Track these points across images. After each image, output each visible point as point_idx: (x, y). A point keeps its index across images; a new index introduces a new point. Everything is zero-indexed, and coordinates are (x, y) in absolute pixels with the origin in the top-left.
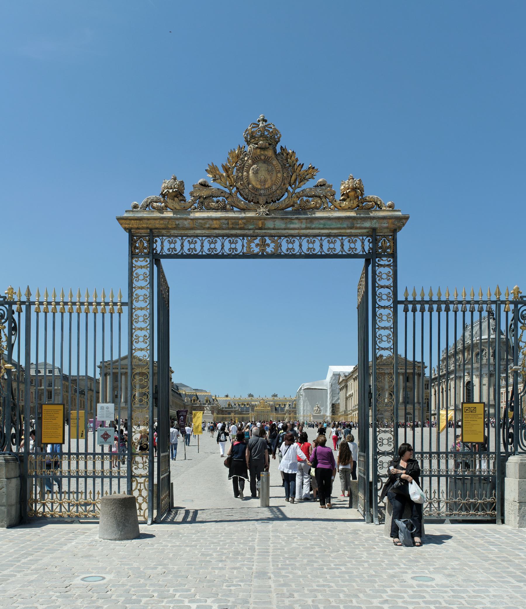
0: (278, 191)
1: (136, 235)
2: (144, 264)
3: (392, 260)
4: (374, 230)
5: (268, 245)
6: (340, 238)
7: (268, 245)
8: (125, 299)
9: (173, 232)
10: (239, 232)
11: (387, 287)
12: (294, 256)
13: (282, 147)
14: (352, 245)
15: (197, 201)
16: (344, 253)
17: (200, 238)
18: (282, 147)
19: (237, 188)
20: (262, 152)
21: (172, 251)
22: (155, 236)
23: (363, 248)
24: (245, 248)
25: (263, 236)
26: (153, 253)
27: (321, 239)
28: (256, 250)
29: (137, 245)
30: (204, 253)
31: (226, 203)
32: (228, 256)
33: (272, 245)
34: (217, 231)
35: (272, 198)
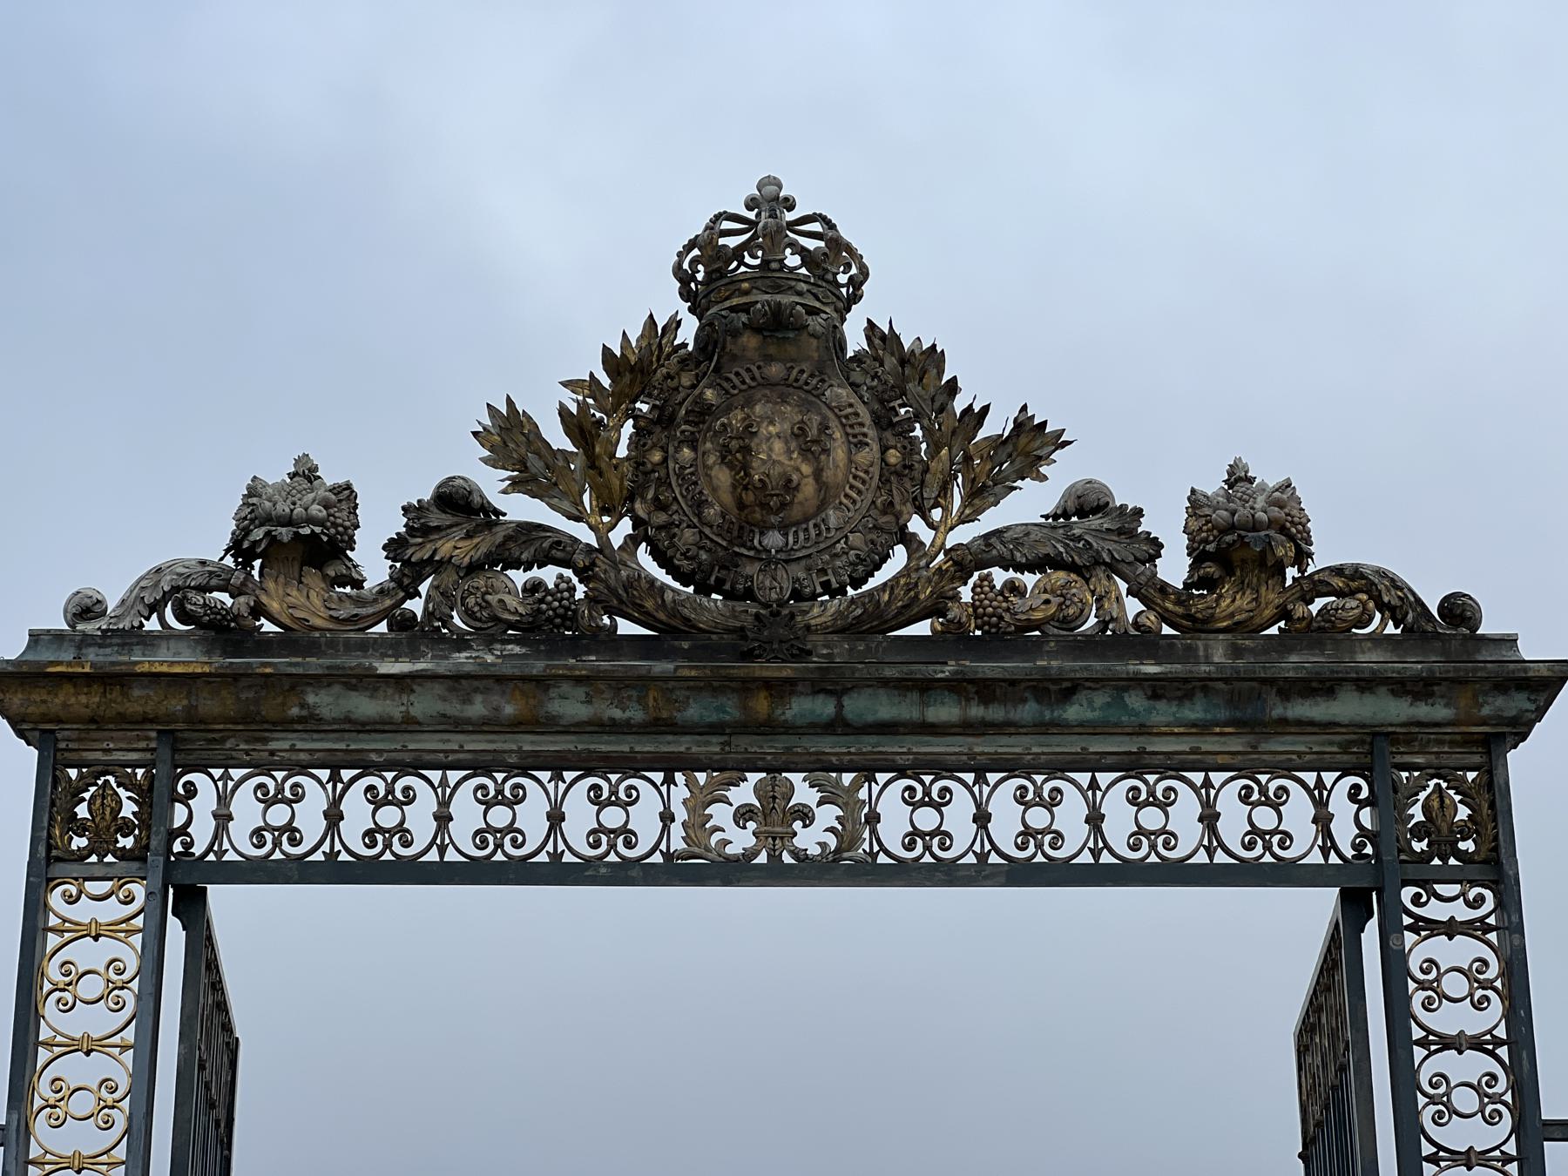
1: (73, 756)
2: (112, 911)
5: (806, 816)
7: (806, 816)
10: (646, 746)
11: (1477, 1044)
12: (948, 874)
13: (871, 326)
14: (1265, 818)
15: (424, 588)
16: (1221, 858)
17: (435, 776)
18: (871, 326)
19: (637, 523)
21: (277, 844)
23: (1328, 834)
24: (677, 830)
26: (170, 850)
28: (741, 840)
29: (82, 811)
30: (451, 856)
31: (579, 595)
32: (585, 873)
33: (828, 815)
34: (529, 743)
35: (823, 571)
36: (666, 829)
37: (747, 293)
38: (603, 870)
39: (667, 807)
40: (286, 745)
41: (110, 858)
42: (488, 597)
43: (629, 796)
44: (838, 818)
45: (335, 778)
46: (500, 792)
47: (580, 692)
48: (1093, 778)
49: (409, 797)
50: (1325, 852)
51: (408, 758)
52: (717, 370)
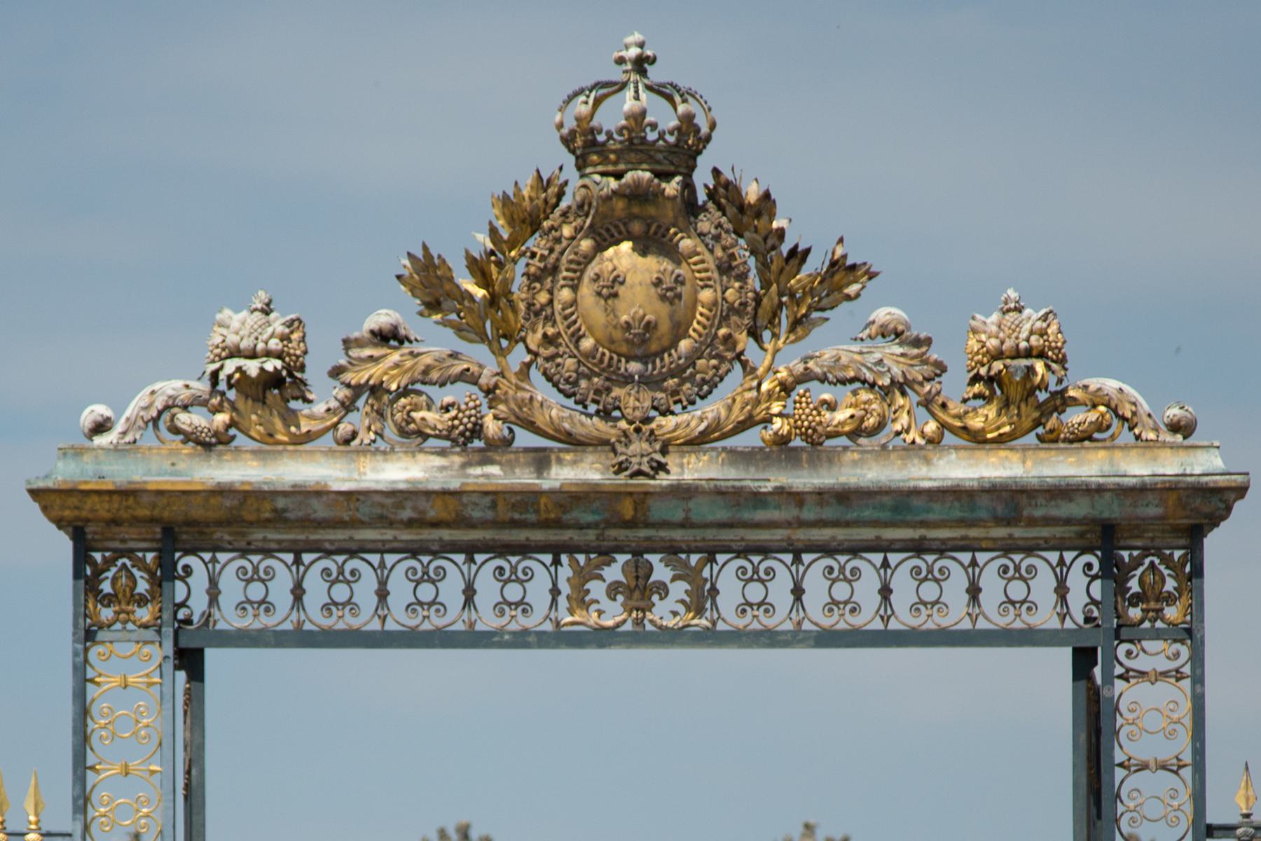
1: (99, 545)
3: (1185, 652)
5: (662, 589)
6: (966, 557)
9: (257, 535)
10: (538, 536)
12: (769, 638)
13: (716, 172)
14: (1017, 590)
15: (360, 403)
16: (982, 624)
17: (375, 558)
18: (716, 172)
20: (636, 210)
22: (187, 552)
24: (562, 601)
25: (637, 553)
27: (885, 564)
33: (679, 590)
34: (447, 534)
36: (554, 601)
37: (615, 163)
38: (507, 637)
39: (555, 584)
41: (130, 626)
42: (413, 414)
43: (526, 574)
44: (686, 592)
45: (298, 561)
46: (426, 573)
48: (885, 559)
50: (1063, 618)
51: (354, 546)
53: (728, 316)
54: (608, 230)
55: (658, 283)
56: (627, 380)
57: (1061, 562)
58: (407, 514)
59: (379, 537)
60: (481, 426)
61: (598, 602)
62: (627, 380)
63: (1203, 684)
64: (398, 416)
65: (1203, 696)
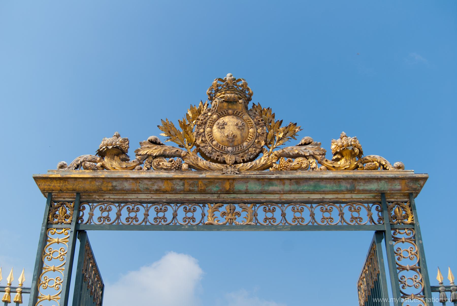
0: (250, 149)
1: (56, 200)
4: (383, 194)
5: (239, 214)
7: (239, 214)
8: (29, 284)
10: (198, 197)
13: (254, 104)
17: (145, 205)
18: (254, 104)
29: (57, 213)
30: (148, 224)
34: (168, 196)
35: (242, 157)
36: (203, 217)
38: (187, 227)
40: (108, 197)
47: (181, 183)
48: (311, 205)
49: (138, 210)
51: (138, 200)
52: (217, 111)
53: (258, 136)
54: (222, 112)
55: (237, 125)
56: (227, 153)
57: (368, 206)
58: (155, 187)
59: (146, 197)
60: (181, 167)
61: (217, 217)
62: (227, 153)
63: (421, 240)
64: (155, 164)
65: (422, 244)
